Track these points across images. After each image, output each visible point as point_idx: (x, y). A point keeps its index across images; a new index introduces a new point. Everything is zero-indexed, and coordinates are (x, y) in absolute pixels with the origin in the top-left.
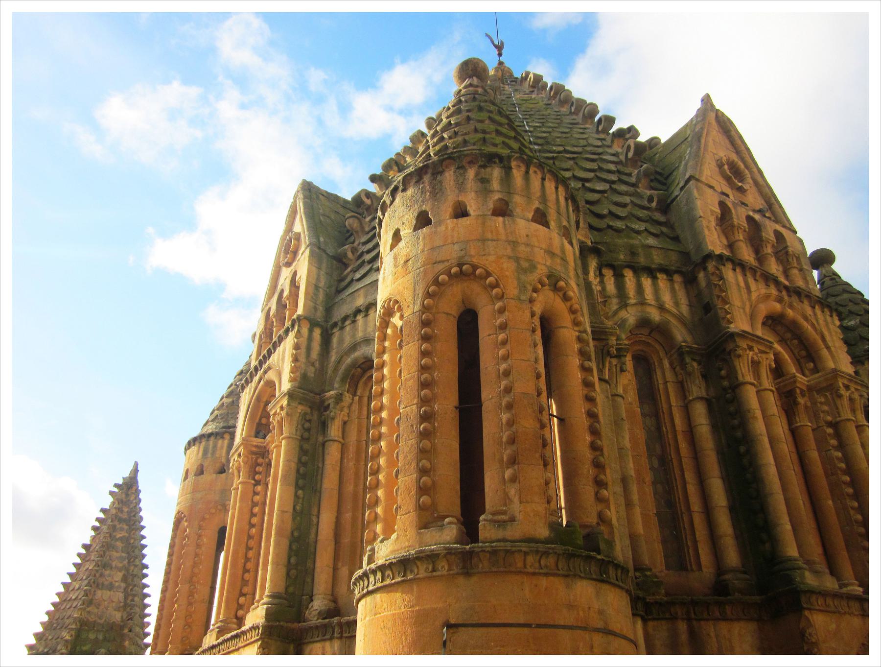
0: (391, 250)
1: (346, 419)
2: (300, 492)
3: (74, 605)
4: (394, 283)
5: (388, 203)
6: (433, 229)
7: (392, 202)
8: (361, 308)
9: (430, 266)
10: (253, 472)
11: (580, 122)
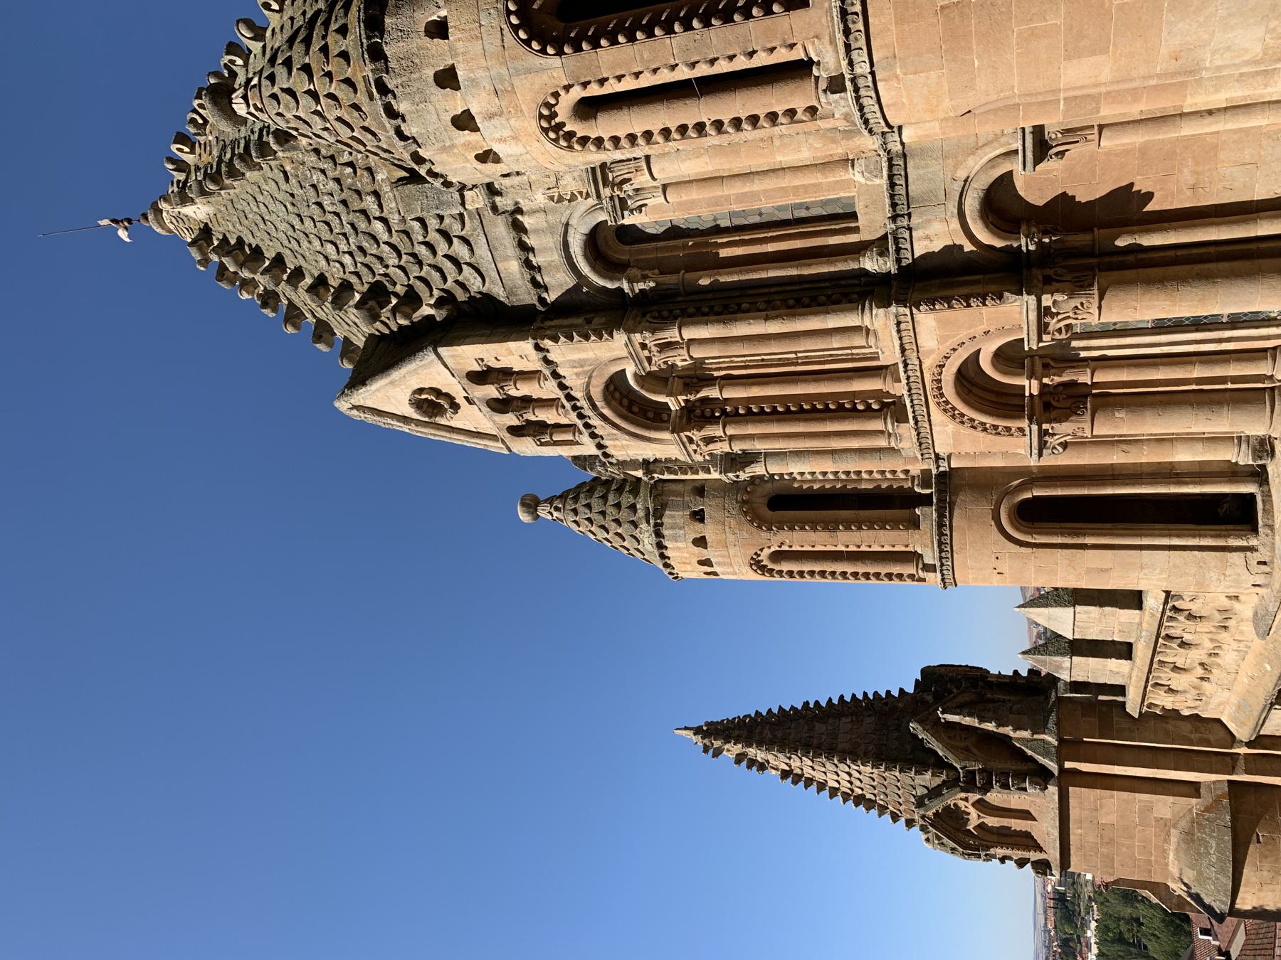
0: (476, 129)
1: (656, 271)
2: (745, 306)
3: (857, 775)
4: (521, 111)
5: (414, 147)
6: (460, 58)
7: (415, 141)
8: (523, 258)
9: (506, 53)
10: (712, 420)
11: (262, 44)
